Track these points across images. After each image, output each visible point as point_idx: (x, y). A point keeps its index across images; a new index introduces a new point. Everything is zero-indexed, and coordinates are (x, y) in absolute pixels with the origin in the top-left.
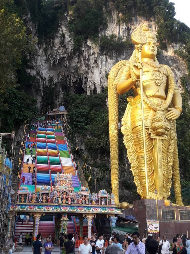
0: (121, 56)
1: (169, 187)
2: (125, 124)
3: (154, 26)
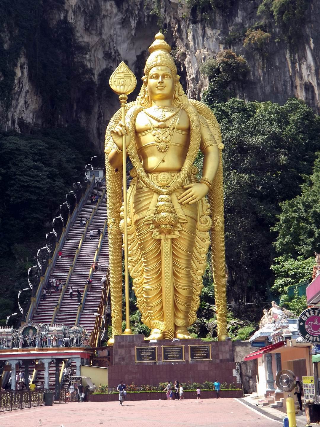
0: (232, 19)
1: (194, 308)
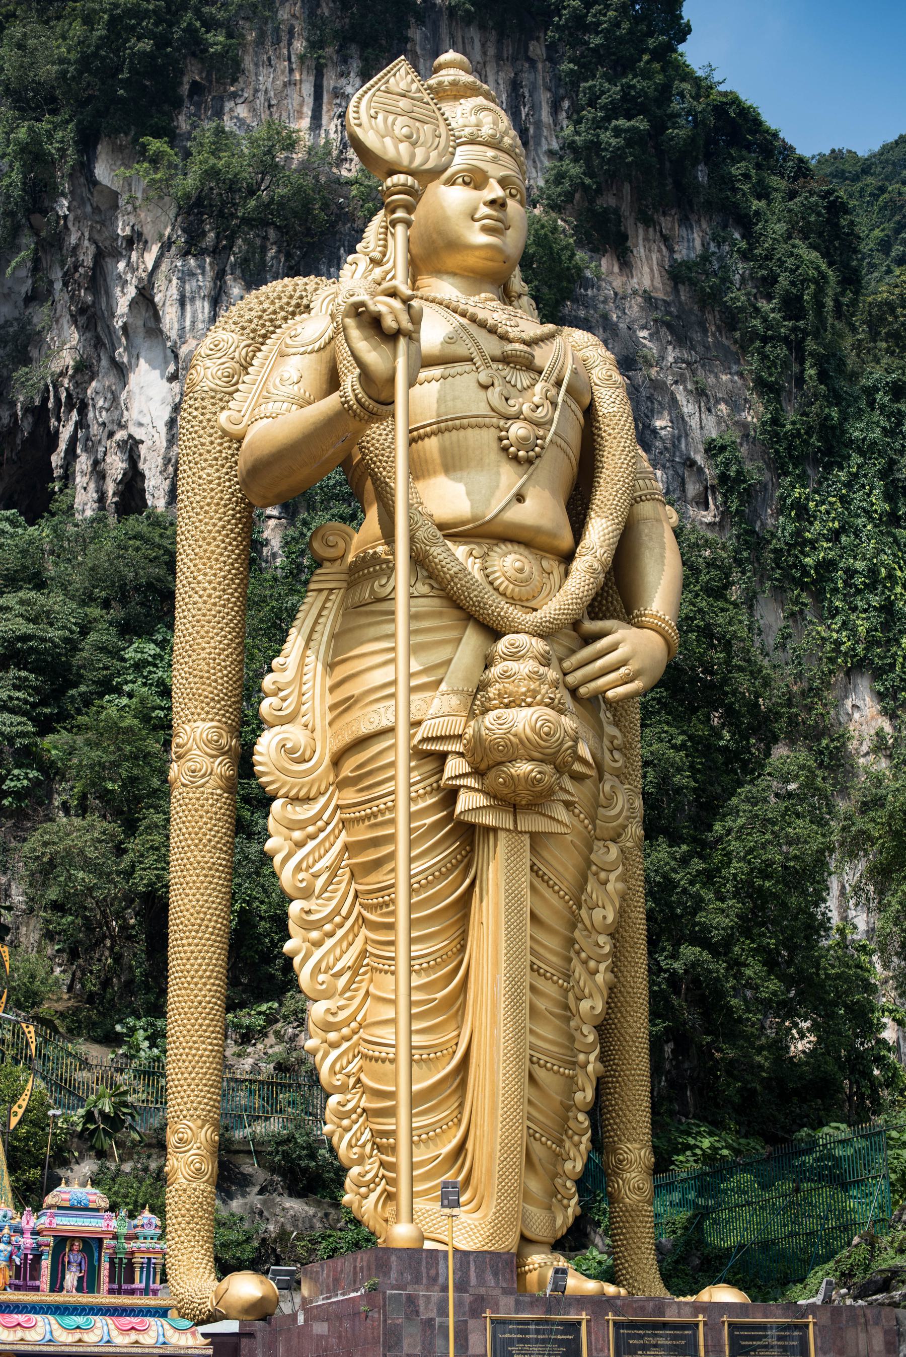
1: (568, 1166)
2: (290, 719)
3: (549, 95)
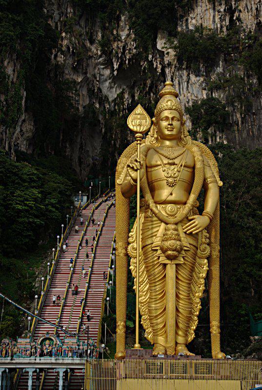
1: (192, 328)
